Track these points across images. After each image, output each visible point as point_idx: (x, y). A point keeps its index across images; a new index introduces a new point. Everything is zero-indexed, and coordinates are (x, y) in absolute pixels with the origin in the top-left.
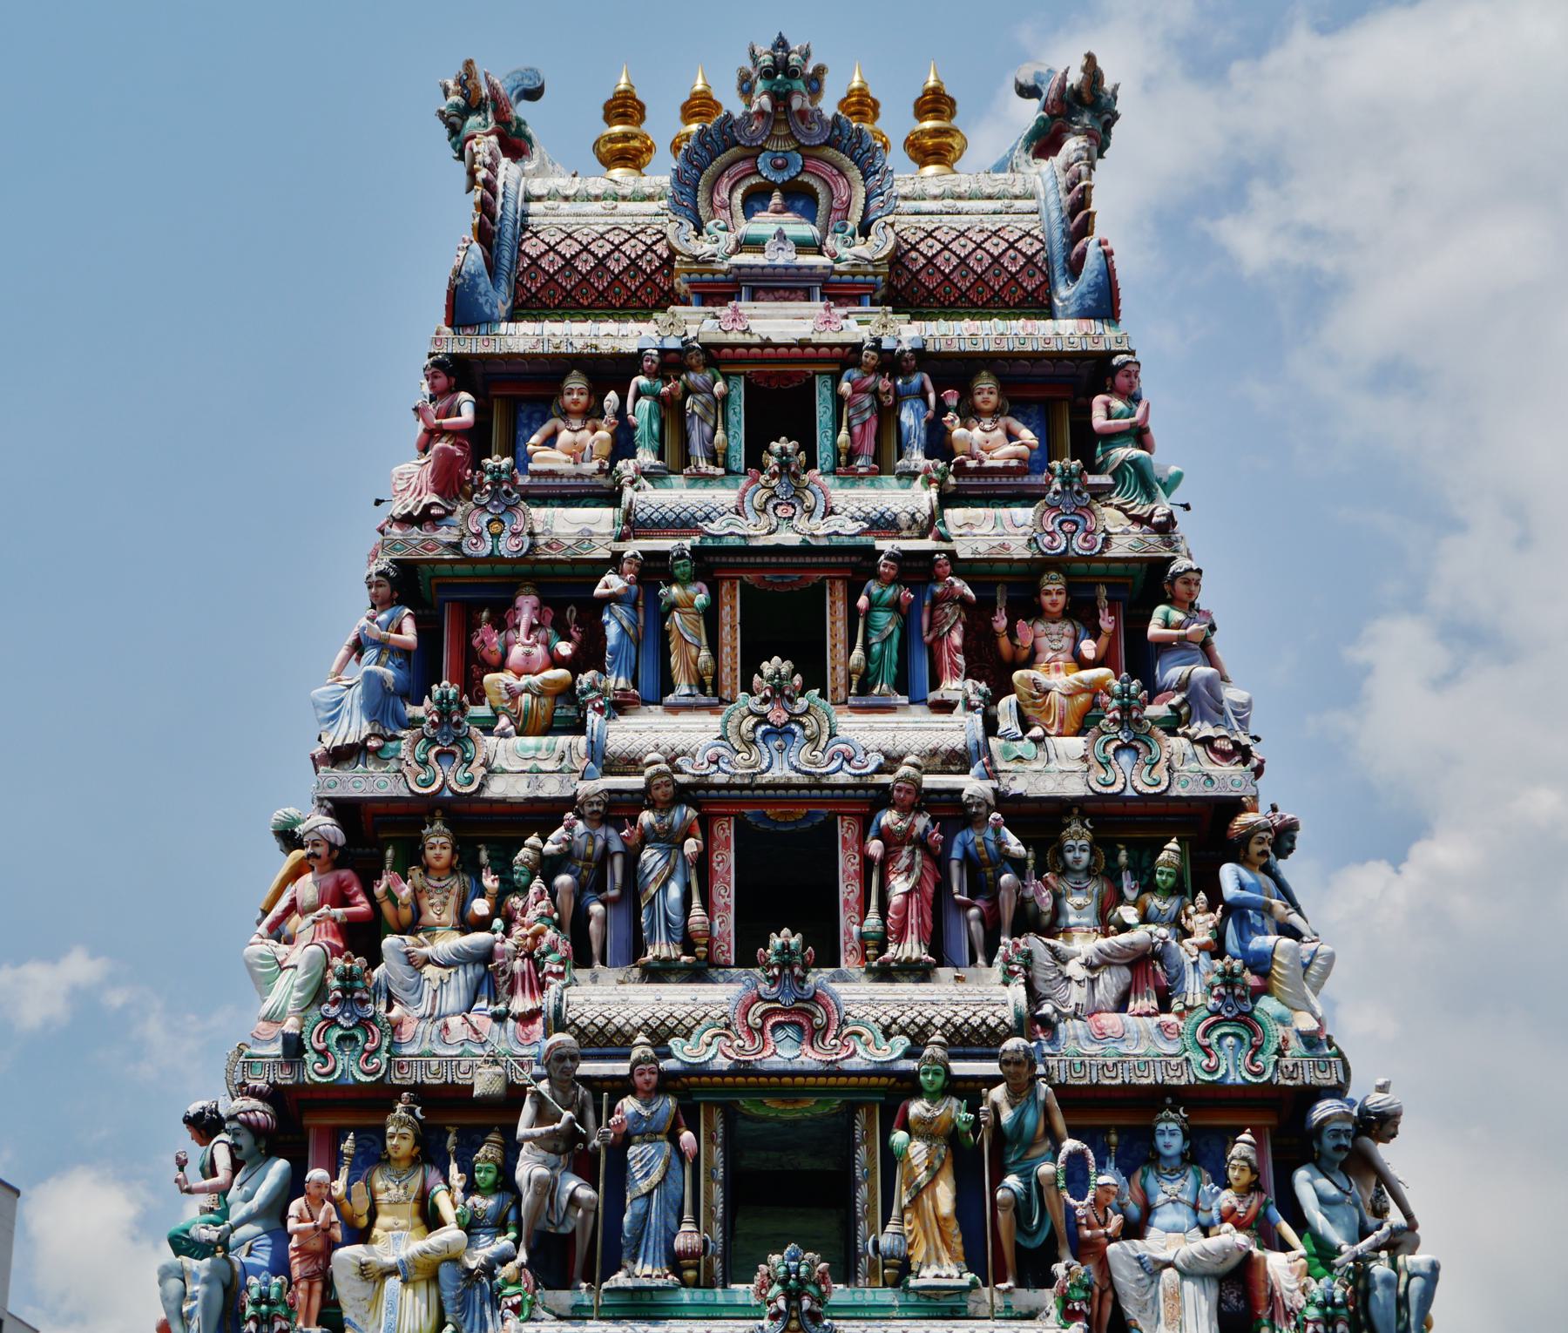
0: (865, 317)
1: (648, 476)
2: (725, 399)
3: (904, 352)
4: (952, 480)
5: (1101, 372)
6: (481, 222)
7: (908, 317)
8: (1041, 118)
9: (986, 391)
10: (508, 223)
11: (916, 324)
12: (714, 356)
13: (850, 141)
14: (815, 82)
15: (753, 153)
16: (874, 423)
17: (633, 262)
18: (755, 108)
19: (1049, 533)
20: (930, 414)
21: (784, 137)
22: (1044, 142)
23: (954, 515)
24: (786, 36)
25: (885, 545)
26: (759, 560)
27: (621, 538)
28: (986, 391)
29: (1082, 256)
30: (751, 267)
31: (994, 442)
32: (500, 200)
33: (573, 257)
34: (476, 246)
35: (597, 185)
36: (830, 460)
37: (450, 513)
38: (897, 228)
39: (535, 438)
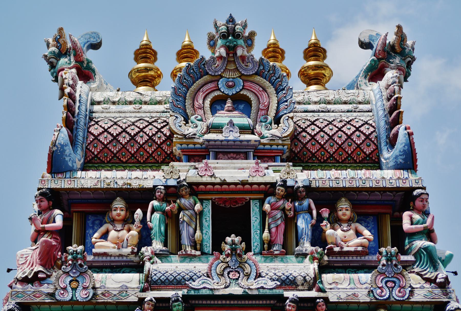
0: (277, 168)
1: (158, 255)
2: (201, 213)
3: (299, 187)
4: (326, 258)
5: (407, 198)
6: (67, 117)
7: (301, 168)
8: (373, 60)
9: (344, 209)
10: (82, 117)
11: (306, 172)
12: (195, 189)
13: (269, 72)
14: (250, 40)
15: (216, 79)
16: (283, 227)
17: (150, 138)
18: (217, 54)
19: (380, 288)
20: (314, 221)
21: (232, 70)
22: (375, 73)
23: (327, 278)
24: (234, 16)
25: (289, 294)
26: (220, 302)
27: (144, 290)
28: (344, 209)
29: (396, 135)
30: (215, 141)
31: (349, 237)
32: (78, 104)
33: (117, 135)
34: (64, 129)
35: (131, 96)
36: (259, 247)
37: (49, 276)
38: (295, 120)
39: (96, 235)
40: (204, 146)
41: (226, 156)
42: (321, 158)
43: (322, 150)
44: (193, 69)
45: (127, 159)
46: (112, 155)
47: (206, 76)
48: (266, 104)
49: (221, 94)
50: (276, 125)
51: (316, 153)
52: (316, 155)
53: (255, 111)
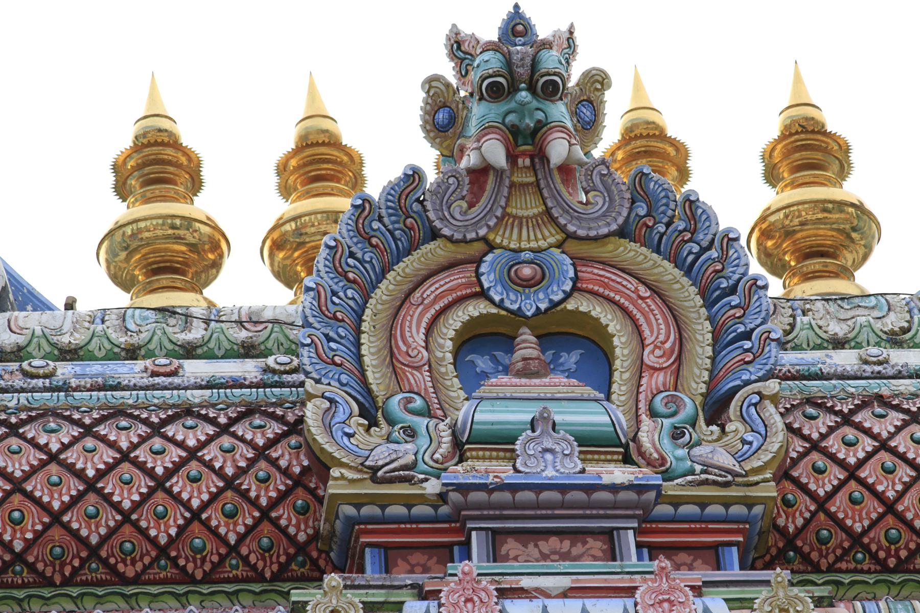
17: (230, 483)
24: (528, 11)
33: (101, 474)
40: (444, 510)
41: (531, 546)
42: (889, 555)
43: (890, 520)
44: (380, 219)
45: (139, 566)
46: (84, 554)
47: (432, 245)
48: (668, 345)
49: (494, 310)
50: (714, 428)
51: (865, 532)
52: (866, 540)
53: (626, 376)
